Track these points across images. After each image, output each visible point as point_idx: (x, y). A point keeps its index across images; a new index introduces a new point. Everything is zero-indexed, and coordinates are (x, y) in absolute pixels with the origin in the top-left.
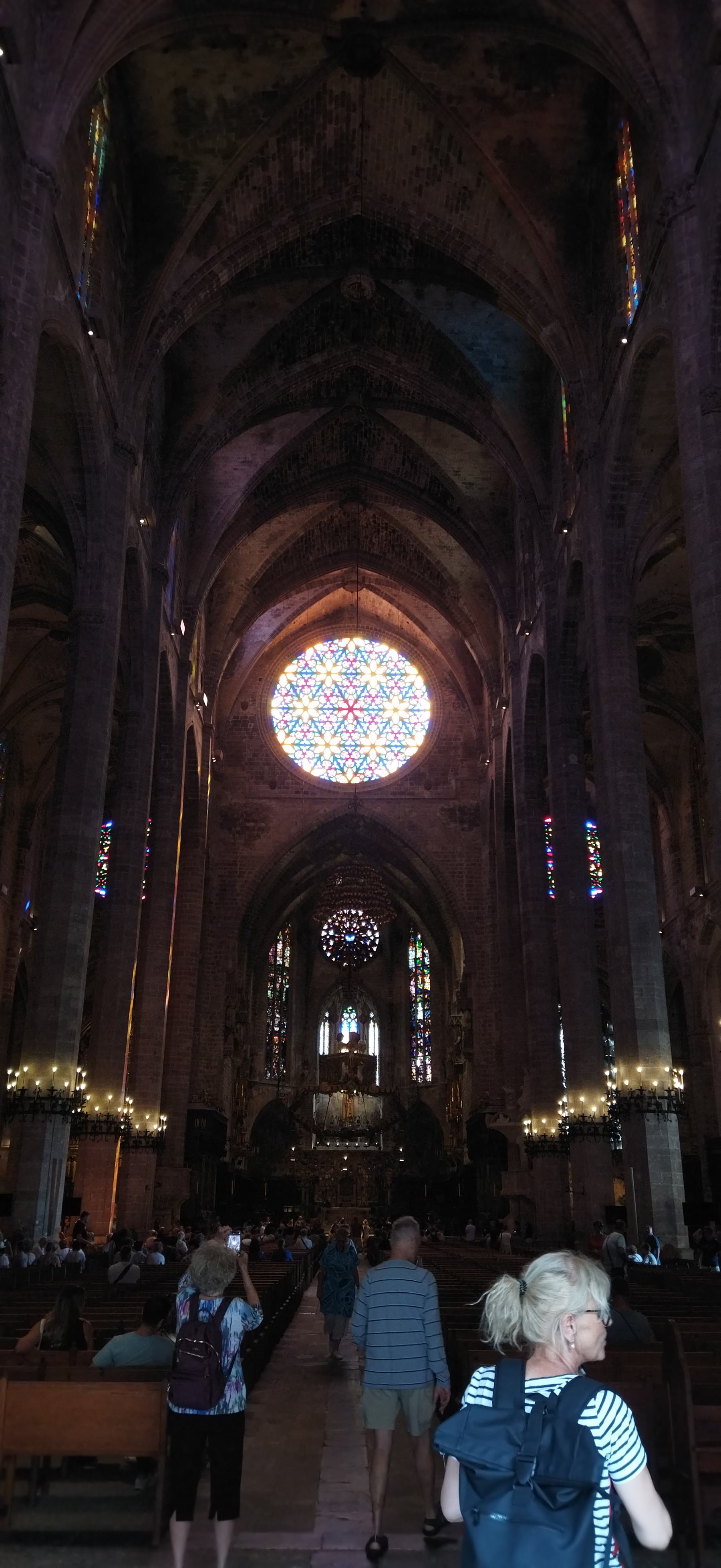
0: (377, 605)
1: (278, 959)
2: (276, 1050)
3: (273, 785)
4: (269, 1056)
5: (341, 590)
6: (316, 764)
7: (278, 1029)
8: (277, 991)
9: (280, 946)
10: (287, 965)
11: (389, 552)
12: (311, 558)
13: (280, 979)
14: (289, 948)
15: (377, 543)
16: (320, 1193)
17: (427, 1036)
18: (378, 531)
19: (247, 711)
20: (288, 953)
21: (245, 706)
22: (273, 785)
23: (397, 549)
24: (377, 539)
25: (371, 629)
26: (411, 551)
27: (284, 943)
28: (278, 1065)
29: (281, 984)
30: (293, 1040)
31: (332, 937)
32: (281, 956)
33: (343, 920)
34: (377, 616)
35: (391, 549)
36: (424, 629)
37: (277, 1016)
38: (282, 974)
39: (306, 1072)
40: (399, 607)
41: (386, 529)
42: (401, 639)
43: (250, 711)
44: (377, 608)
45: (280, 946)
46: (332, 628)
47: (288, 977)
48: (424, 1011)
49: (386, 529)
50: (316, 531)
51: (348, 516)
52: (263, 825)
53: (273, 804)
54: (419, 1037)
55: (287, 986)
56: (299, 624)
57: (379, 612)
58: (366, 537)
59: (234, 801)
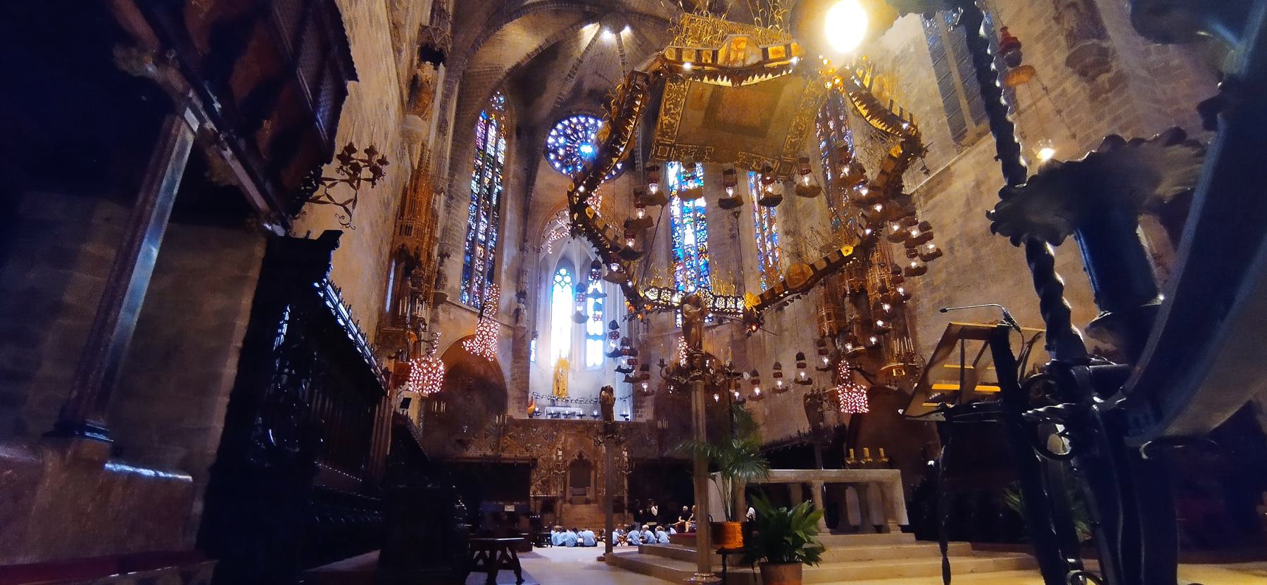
1: (488, 146)
2: (479, 265)
4: (468, 271)
7: (484, 238)
8: (485, 187)
9: (492, 132)
10: (501, 160)
13: (490, 173)
14: (504, 142)
16: (539, 482)
17: (701, 263)
20: (502, 145)
27: (498, 129)
28: (481, 287)
29: (491, 181)
30: (505, 259)
31: (564, 147)
32: (494, 145)
33: (577, 128)
37: (484, 219)
38: (493, 170)
39: (522, 306)
45: (492, 132)
47: (501, 177)
48: (695, 233)
54: (688, 267)
55: (500, 188)
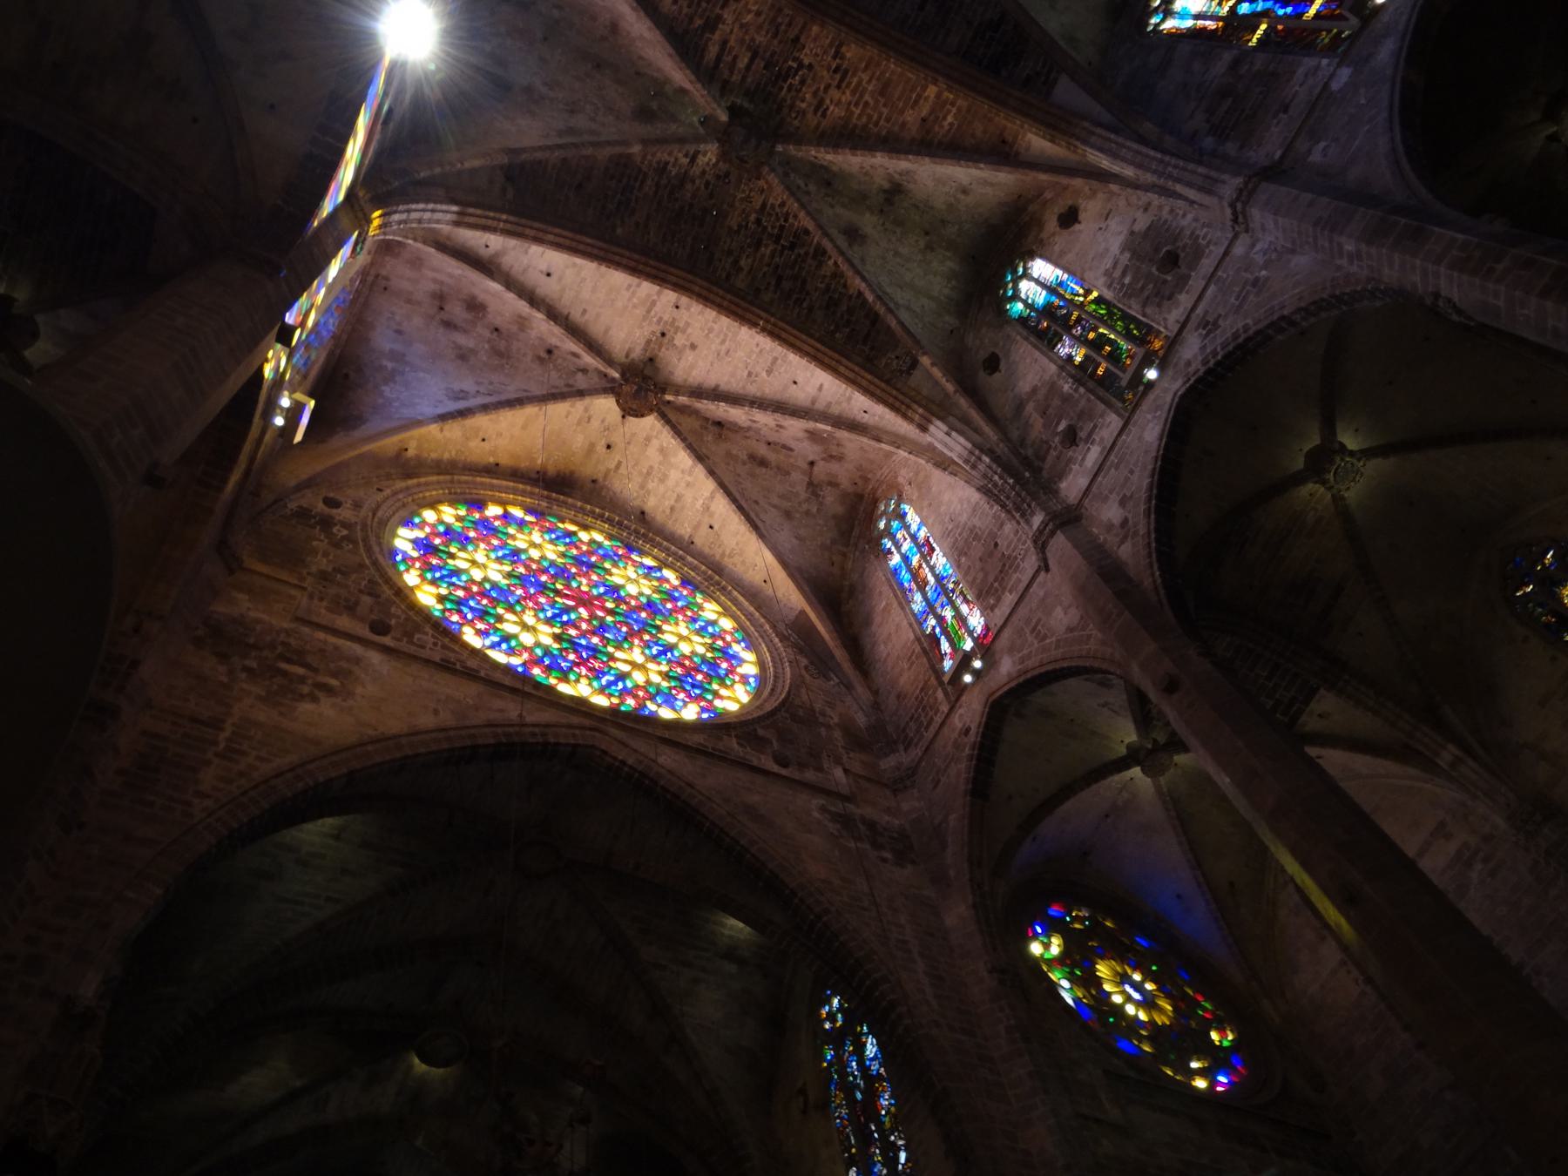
0: (651, 485)
3: (380, 628)
5: (606, 406)
6: (498, 644)
11: (767, 289)
12: (619, 231)
15: (745, 272)
18: (758, 245)
19: (334, 511)
21: (332, 503)
22: (380, 628)
23: (786, 285)
24: (750, 261)
25: (628, 528)
26: (817, 289)
34: (643, 513)
35: (773, 283)
36: (755, 527)
40: (711, 473)
41: (777, 241)
42: (689, 559)
43: (345, 513)
44: (648, 492)
46: (548, 497)
49: (777, 241)
50: (649, 182)
51: (711, 196)
52: (334, 682)
53: (375, 657)
56: (492, 453)
57: (651, 504)
58: (730, 252)
59: (252, 614)
